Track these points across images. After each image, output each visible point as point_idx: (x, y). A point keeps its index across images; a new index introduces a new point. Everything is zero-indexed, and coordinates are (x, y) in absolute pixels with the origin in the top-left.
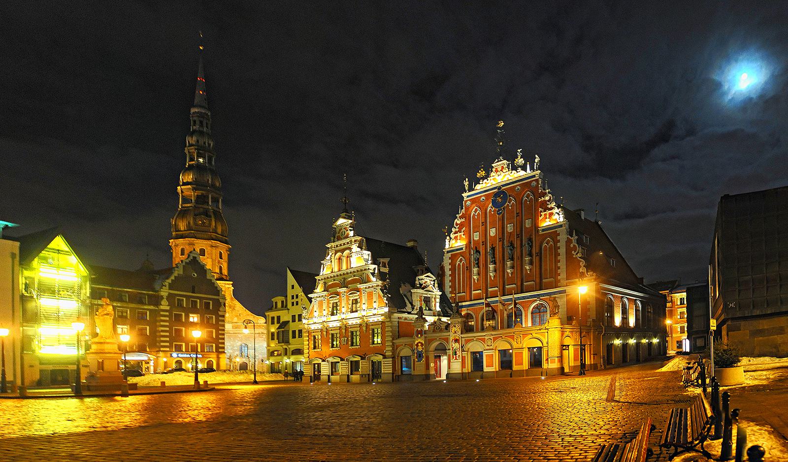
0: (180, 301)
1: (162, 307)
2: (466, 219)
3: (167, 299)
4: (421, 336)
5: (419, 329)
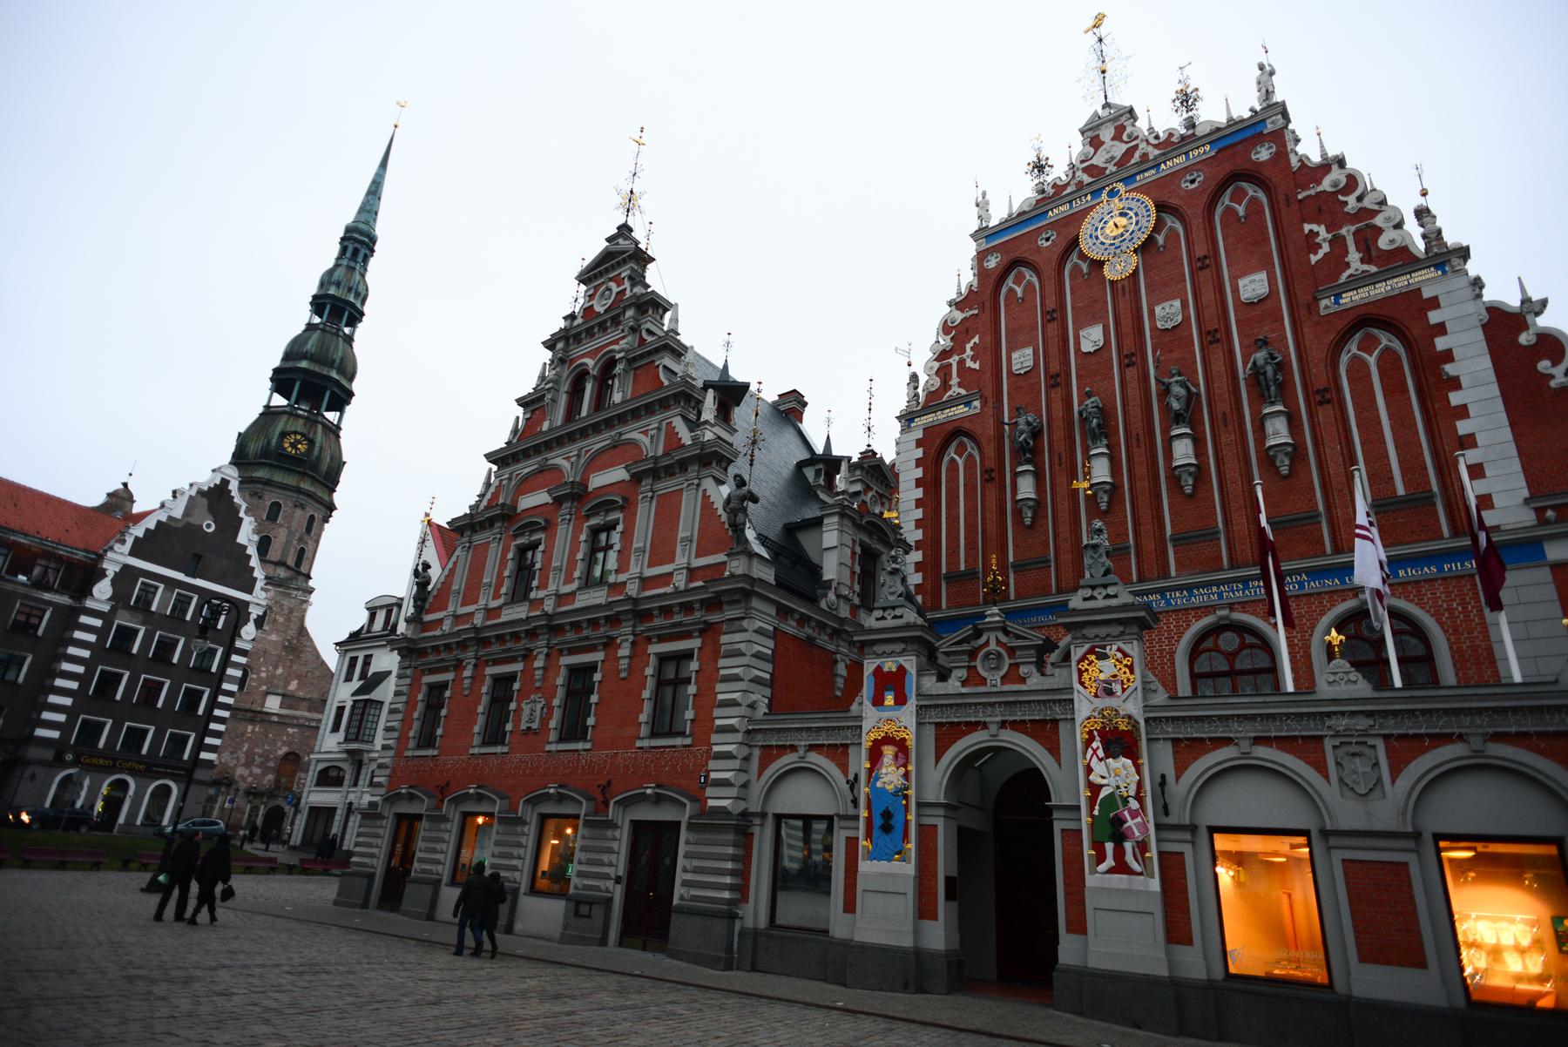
0: (148, 592)
1: (89, 604)
2: (982, 308)
3: (114, 582)
4: (901, 700)
5: (890, 665)
